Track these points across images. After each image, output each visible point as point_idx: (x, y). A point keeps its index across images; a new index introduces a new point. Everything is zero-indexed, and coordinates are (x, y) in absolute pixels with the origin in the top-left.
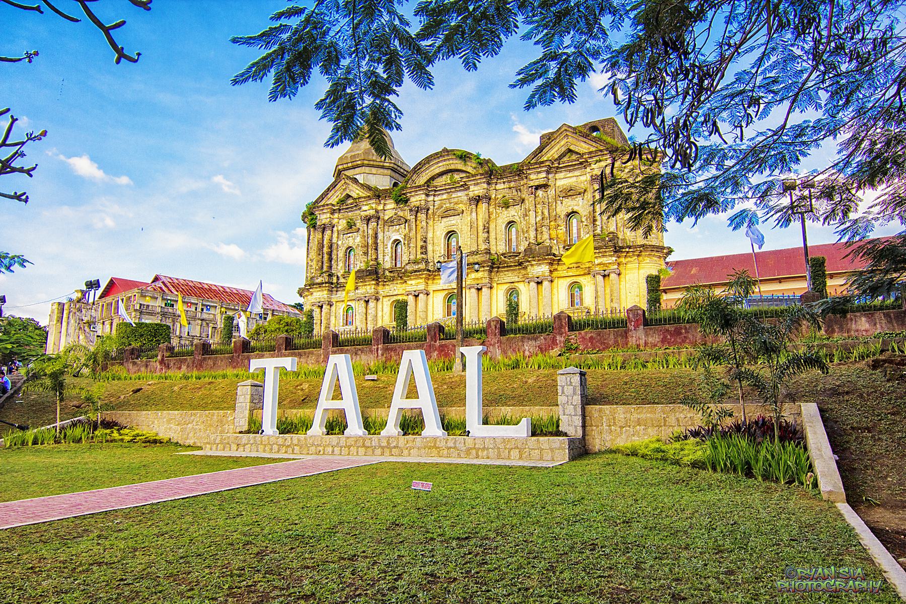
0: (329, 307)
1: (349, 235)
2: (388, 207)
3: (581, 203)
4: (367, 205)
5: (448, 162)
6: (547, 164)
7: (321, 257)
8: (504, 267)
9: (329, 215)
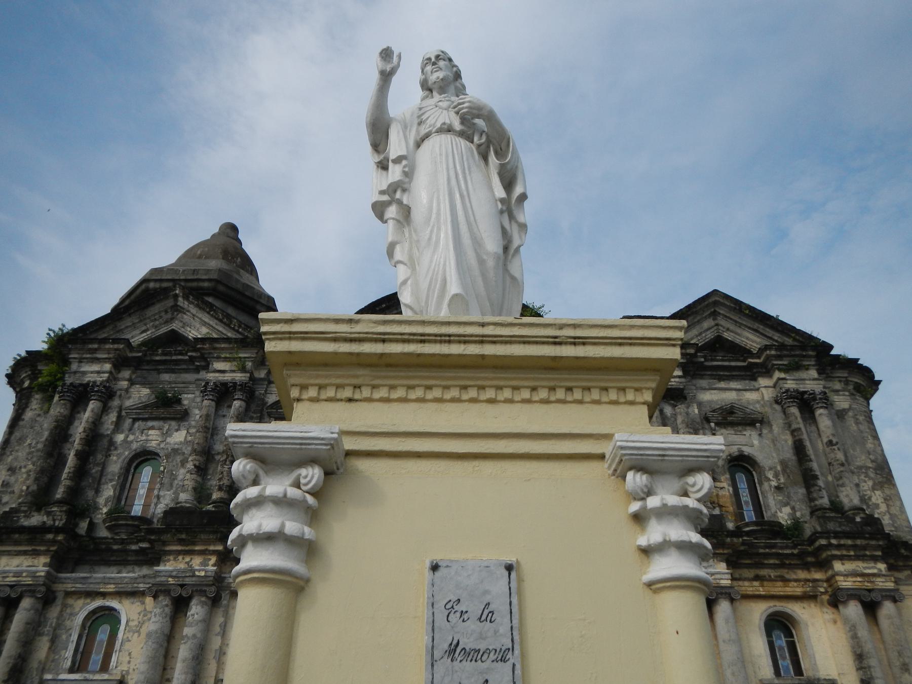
0: (40, 606)
1: (150, 424)
3: (756, 442)
4: (234, 359)
7: (51, 461)
9: (108, 367)
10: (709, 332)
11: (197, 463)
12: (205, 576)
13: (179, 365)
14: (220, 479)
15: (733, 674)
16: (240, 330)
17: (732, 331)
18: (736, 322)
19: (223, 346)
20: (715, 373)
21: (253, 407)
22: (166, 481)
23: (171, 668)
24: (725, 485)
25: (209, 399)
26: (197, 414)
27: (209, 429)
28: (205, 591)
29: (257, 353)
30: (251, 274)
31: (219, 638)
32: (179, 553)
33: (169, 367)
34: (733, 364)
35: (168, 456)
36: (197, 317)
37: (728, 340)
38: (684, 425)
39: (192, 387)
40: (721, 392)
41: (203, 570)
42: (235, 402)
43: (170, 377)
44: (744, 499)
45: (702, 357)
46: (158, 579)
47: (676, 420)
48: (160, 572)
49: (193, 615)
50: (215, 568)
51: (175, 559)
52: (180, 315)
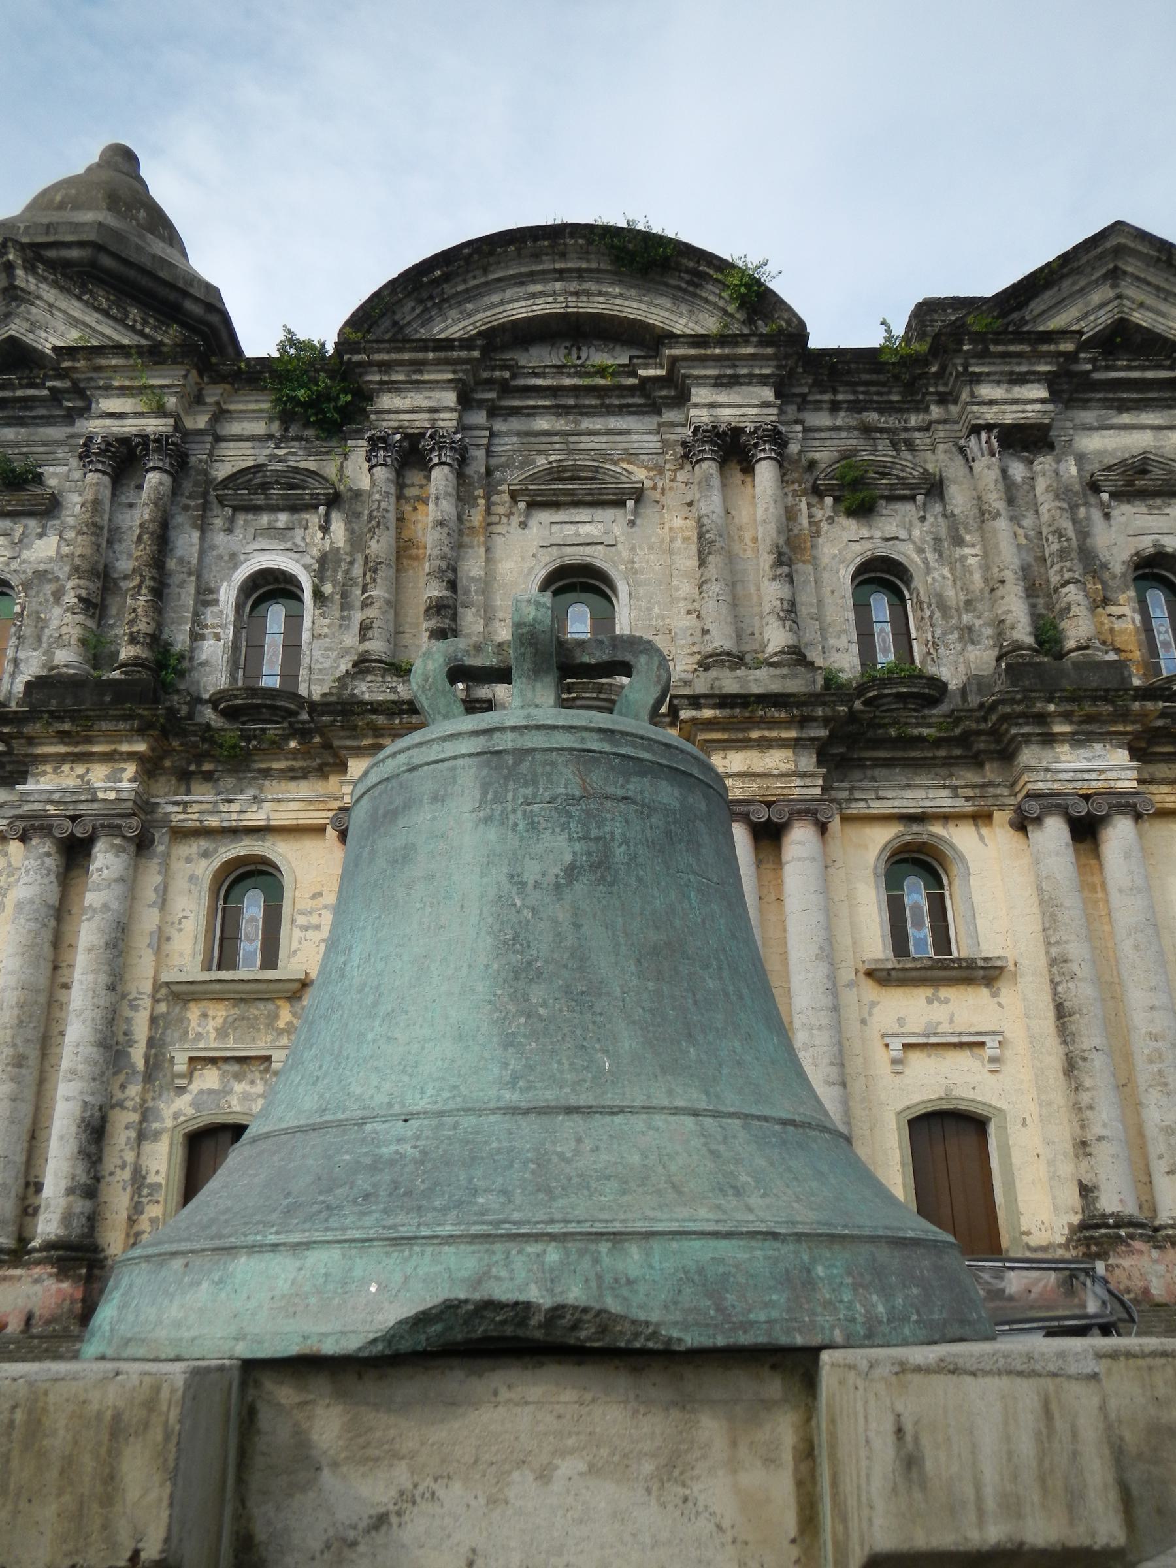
2: (235, 428)
4: (141, 390)
5: (573, 286)
6: (1068, 347)
8: (878, 743)
10: (1102, 312)
11: (84, 593)
12: (118, 800)
13: (31, 408)
14: (132, 623)
15: (1136, 947)
16: (147, 330)
17: (1150, 309)
18: (1158, 288)
19: (114, 362)
20: (1111, 396)
21: (188, 486)
22: (27, 631)
23: (70, 966)
24: (1126, 610)
25: (97, 471)
26: (75, 504)
27: (101, 528)
28: (119, 827)
29: (185, 377)
30: (171, 245)
31: (156, 910)
32: (62, 758)
33: (11, 413)
34: (1150, 374)
35: (26, 586)
36: (59, 309)
37: (1139, 326)
38: (1051, 495)
39: (62, 453)
40: (1122, 433)
41: (112, 789)
42: (150, 475)
43: (18, 434)
44: (1162, 637)
45: (1089, 361)
46: (27, 807)
47: (1033, 488)
48: (29, 793)
49: (100, 870)
50: (135, 785)
51: (55, 770)
52: (22, 308)
